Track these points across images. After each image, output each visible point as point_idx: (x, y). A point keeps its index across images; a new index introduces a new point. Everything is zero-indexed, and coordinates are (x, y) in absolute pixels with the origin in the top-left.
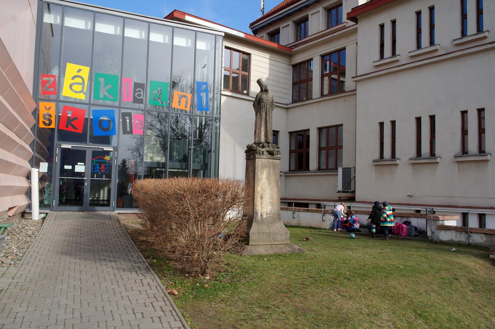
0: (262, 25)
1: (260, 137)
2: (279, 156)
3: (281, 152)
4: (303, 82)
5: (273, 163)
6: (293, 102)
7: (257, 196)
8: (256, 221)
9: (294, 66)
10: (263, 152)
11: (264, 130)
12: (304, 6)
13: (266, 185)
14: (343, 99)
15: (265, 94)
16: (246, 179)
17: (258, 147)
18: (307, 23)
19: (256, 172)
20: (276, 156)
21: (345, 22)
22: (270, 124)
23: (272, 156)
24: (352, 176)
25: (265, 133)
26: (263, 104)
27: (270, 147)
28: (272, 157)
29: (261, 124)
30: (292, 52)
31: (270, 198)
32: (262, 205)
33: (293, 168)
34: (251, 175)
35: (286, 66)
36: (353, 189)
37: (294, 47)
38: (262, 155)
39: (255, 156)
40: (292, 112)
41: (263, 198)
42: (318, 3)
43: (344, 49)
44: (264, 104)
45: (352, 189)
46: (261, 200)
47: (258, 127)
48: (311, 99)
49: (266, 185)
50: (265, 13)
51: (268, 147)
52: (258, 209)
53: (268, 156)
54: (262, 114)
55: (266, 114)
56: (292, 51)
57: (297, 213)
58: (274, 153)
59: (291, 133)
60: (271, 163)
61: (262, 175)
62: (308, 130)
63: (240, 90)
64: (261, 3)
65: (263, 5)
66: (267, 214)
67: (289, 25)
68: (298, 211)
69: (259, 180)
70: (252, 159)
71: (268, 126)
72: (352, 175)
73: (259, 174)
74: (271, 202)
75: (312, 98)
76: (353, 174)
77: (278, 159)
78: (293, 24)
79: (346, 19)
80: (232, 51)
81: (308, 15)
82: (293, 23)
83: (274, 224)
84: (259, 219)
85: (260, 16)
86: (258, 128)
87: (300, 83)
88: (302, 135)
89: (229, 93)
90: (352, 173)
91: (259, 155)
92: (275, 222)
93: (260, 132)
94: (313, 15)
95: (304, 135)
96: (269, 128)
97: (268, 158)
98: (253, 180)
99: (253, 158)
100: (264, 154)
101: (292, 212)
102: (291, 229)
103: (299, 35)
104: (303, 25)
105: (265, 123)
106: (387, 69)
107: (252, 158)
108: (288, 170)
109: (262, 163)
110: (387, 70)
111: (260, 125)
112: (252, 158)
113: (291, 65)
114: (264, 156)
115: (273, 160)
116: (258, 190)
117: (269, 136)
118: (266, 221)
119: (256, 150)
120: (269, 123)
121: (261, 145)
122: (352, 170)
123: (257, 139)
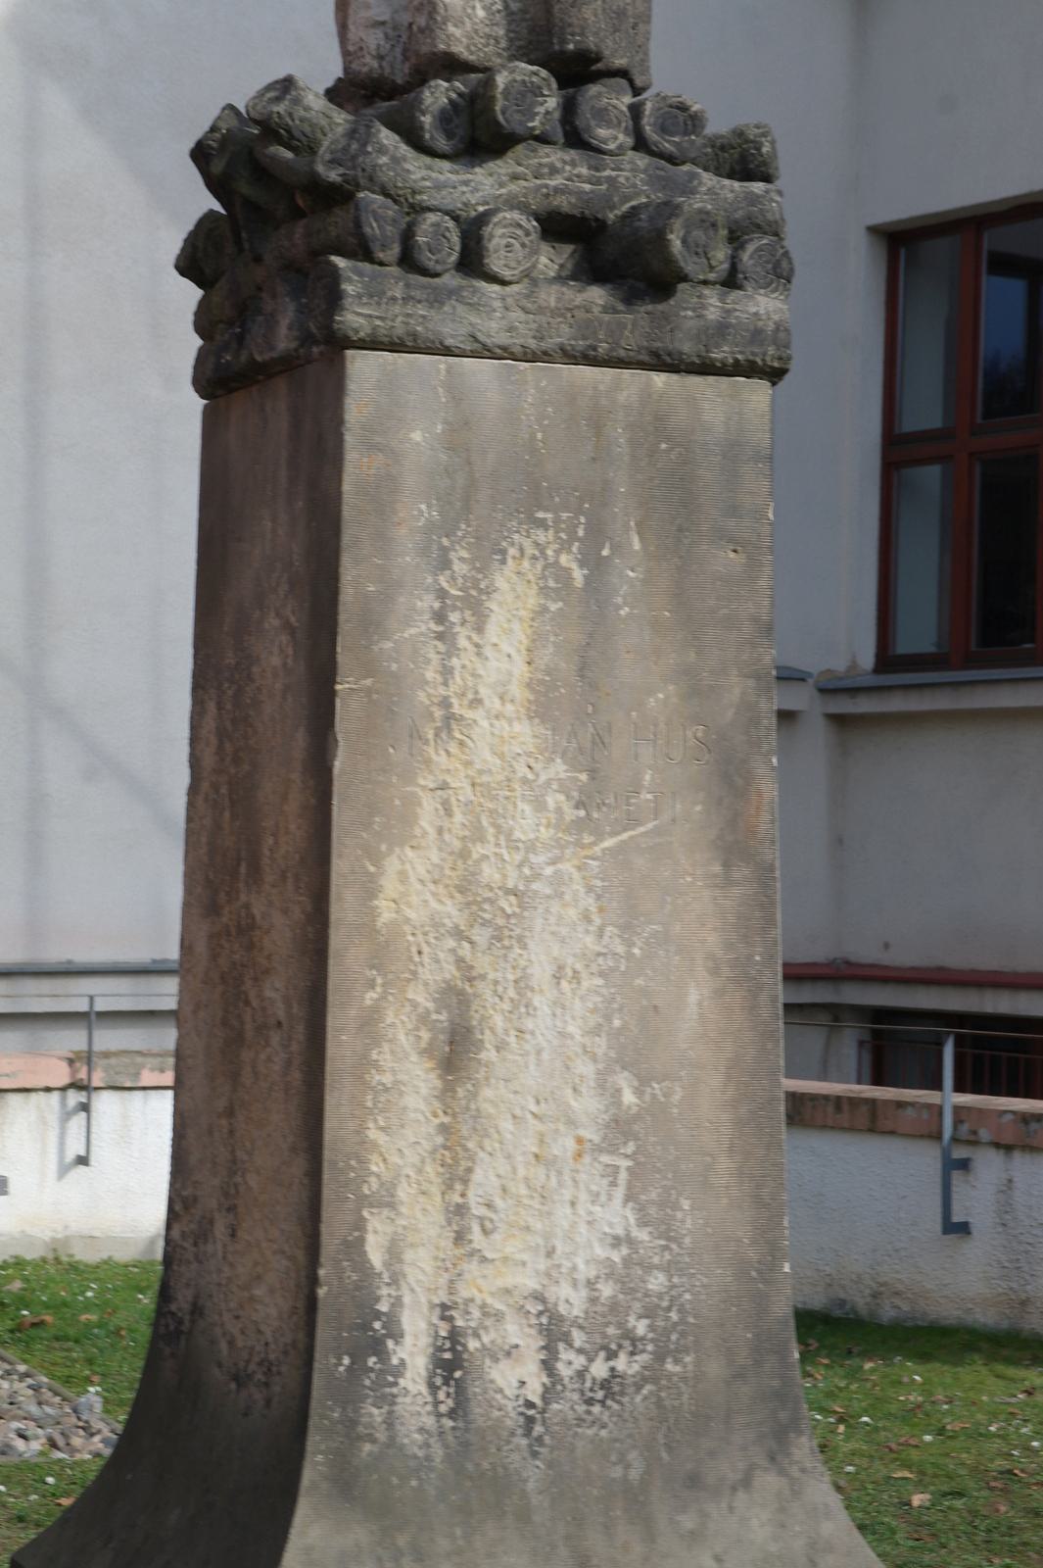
2: (763, 305)
3: (793, 241)
5: (654, 426)
7: (370, 1024)
8: (346, 1483)
10: (473, 233)
13: (526, 823)
16: (210, 723)
17: (386, 136)
19: (348, 594)
20: (714, 305)
23: (631, 299)
27: (612, 136)
28: (635, 326)
31: (601, 1045)
32: (456, 1174)
33: (919, 633)
38: (451, 280)
39: (334, 298)
41: (489, 1054)
46: (447, 1092)
49: (526, 823)
51: (576, 139)
52: (394, 1253)
53: (564, 311)
57: (989, 1167)
60: (619, 435)
61: (453, 650)
66: (553, 1332)
68: (1008, 1149)
69: (416, 735)
70: (287, 365)
74: (620, 1127)
77: (748, 369)
83: (688, 1522)
84: (411, 1437)
91: (395, 281)
92: (694, 1481)
97: (563, 334)
98: (301, 740)
99: (307, 339)
100: (496, 263)
102: (926, 1389)
107: (284, 340)
108: (867, 659)
109: (459, 436)
112: (284, 340)
115: (659, 379)
116: (386, 913)
118: (534, 1474)
119: (338, 196)
121: (438, 95)
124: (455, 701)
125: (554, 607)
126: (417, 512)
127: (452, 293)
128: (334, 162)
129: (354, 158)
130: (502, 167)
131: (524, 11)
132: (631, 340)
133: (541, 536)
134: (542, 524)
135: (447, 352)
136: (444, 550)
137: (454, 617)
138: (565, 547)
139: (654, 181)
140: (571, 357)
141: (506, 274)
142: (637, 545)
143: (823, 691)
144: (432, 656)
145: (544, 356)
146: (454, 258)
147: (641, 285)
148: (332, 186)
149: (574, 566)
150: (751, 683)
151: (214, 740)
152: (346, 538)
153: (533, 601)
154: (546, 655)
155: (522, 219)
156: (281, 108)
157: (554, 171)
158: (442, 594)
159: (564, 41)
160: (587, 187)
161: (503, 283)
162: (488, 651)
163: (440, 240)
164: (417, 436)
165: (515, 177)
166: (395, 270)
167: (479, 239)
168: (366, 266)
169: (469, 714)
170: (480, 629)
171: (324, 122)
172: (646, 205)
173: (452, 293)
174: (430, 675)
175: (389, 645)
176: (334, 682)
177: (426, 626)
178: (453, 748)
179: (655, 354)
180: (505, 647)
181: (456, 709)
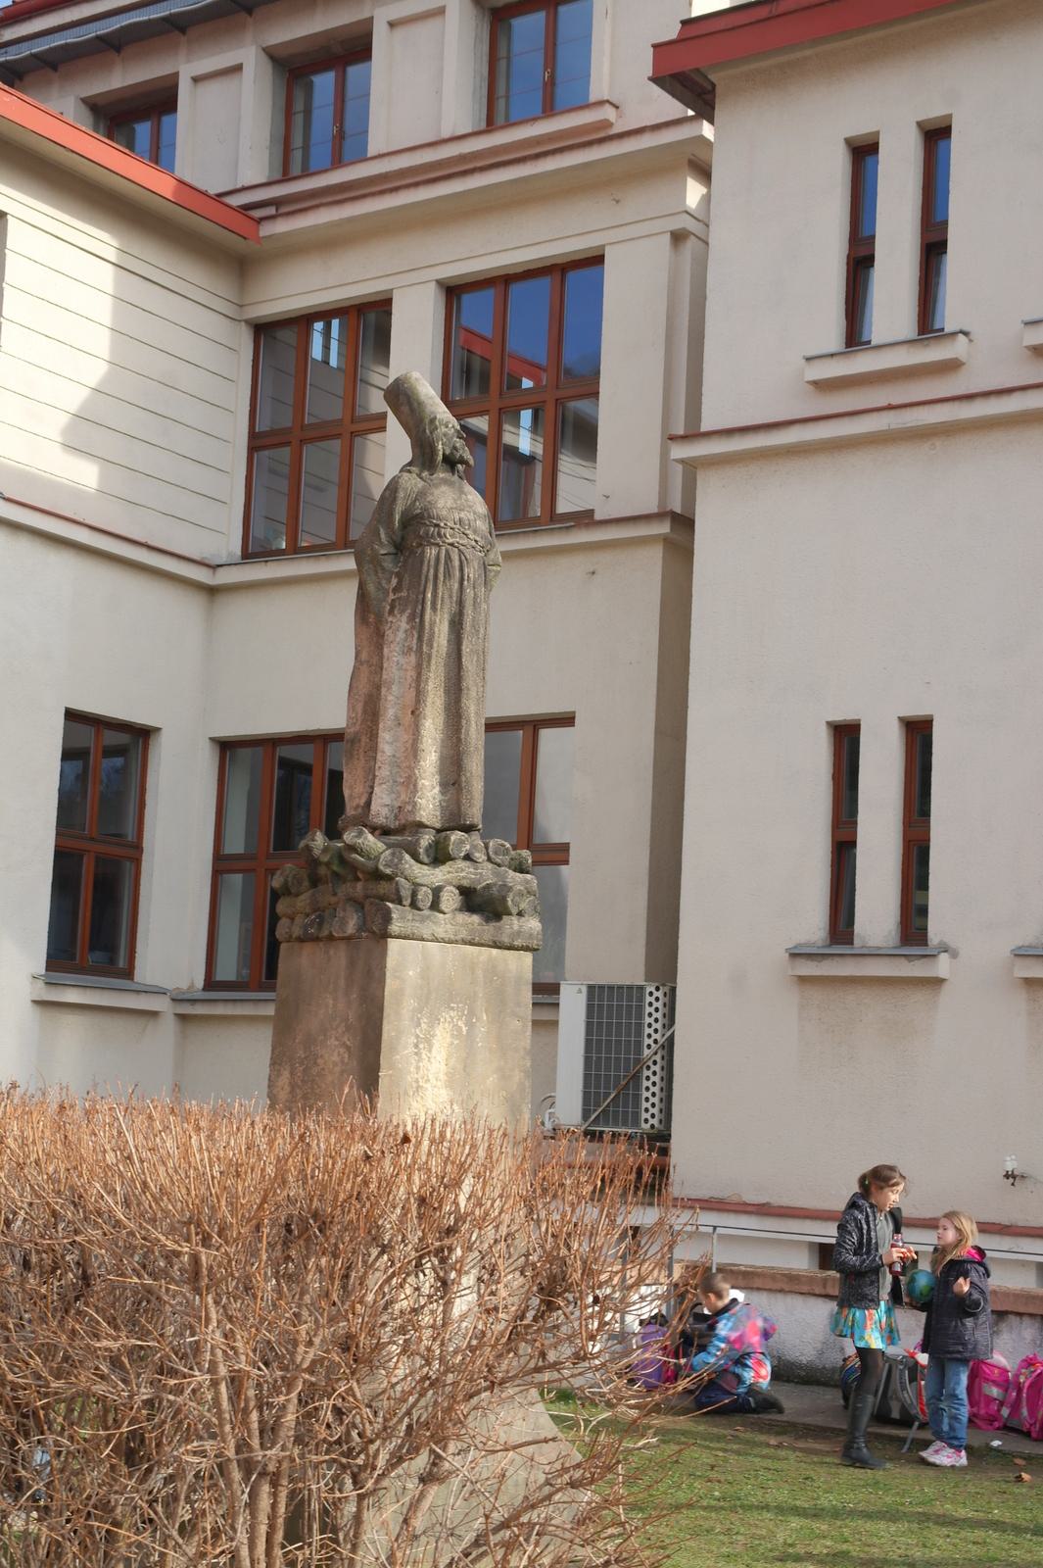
0: (58, 41)
4: (324, 432)
6: (252, 552)
9: (264, 331)
10: (437, 892)
11: (439, 736)
14: (581, 563)
15: (445, 481)
17: (407, 857)
21: (608, 101)
23: (488, 920)
24: (647, 1041)
25: (442, 759)
26: (434, 551)
28: (489, 930)
30: (259, 240)
33: (227, 971)
35: (214, 325)
36: (655, 1122)
37: (271, 211)
38: (427, 912)
40: (238, 612)
43: (596, 260)
45: (649, 1120)
54: (432, 624)
56: (262, 233)
58: (510, 903)
59: (227, 748)
60: (479, 973)
67: (237, 69)
69: (406, 1093)
70: (349, 938)
72: (647, 1031)
76: (658, 1026)
78: (267, 67)
79: (650, 79)
81: (369, 22)
82: (264, 59)
87: (303, 442)
90: (648, 1020)
93: (414, 751)
97: (464, 934)
99: (360, 929)
100: (443, 906)
103: (297, 140)
105: (447, 692)
106: (890, 408)
107: (351, 927)
108: (200, 983)
109: (425, 974)
110: (892, 413)
113: (247, 322)
115: (495, 951)
119: (390, 878)
120: (473, 693)
122: (648, 999)
124: (420, 1080)
125: (456, 1042)
126: (410, 1003)
127: (428, 917)
128: (387, 866)
129: (396, 865)
130: (445, 868)
131: (447, 807)
132: (487, 937)
133: (452, 1013)
134: (452, 1009)
135: (423, 940)
136: (419, 1019)
137: (421, 1046)
138: (460, 1018)
139: (494, 873)
140: (465, 942)
141: (446, 910)
142: (485, 1018)
143: (173, 1000)
144: (413, 1062)
145: (456, 942)
146: (429, 904)
147: (490, 915)
148: (387, 875)
149: (463, 1026)
150: (522, 1074)
151: (287, 1089)
152: (385, 1014)
153: (449, 1040)
154: (452, 1062)
155: (454, 889)
156: (360, 841)
157: (462, 870)
158: (417, 1036)
159: (465, 820)
160: (473, 876)
161: (444, 913)
162: (432, 1060)
163: (425, 896)
164: (411, 973)
165: (449, 872)
166: (408, 908)
167: (439, 897)
168: (399, 907)
169: (425, 1085)
170: (430, 1051)
171: (374, 846)
172: (495, 884)
173: (428, 917)
174: (412, 1069)
175: (398, 1057)
176: (378, 1072)
177: (411, 1049)
178: (419, 1099)
179: (495, 942)
180: (438, 1058)
181: (421, 1084)
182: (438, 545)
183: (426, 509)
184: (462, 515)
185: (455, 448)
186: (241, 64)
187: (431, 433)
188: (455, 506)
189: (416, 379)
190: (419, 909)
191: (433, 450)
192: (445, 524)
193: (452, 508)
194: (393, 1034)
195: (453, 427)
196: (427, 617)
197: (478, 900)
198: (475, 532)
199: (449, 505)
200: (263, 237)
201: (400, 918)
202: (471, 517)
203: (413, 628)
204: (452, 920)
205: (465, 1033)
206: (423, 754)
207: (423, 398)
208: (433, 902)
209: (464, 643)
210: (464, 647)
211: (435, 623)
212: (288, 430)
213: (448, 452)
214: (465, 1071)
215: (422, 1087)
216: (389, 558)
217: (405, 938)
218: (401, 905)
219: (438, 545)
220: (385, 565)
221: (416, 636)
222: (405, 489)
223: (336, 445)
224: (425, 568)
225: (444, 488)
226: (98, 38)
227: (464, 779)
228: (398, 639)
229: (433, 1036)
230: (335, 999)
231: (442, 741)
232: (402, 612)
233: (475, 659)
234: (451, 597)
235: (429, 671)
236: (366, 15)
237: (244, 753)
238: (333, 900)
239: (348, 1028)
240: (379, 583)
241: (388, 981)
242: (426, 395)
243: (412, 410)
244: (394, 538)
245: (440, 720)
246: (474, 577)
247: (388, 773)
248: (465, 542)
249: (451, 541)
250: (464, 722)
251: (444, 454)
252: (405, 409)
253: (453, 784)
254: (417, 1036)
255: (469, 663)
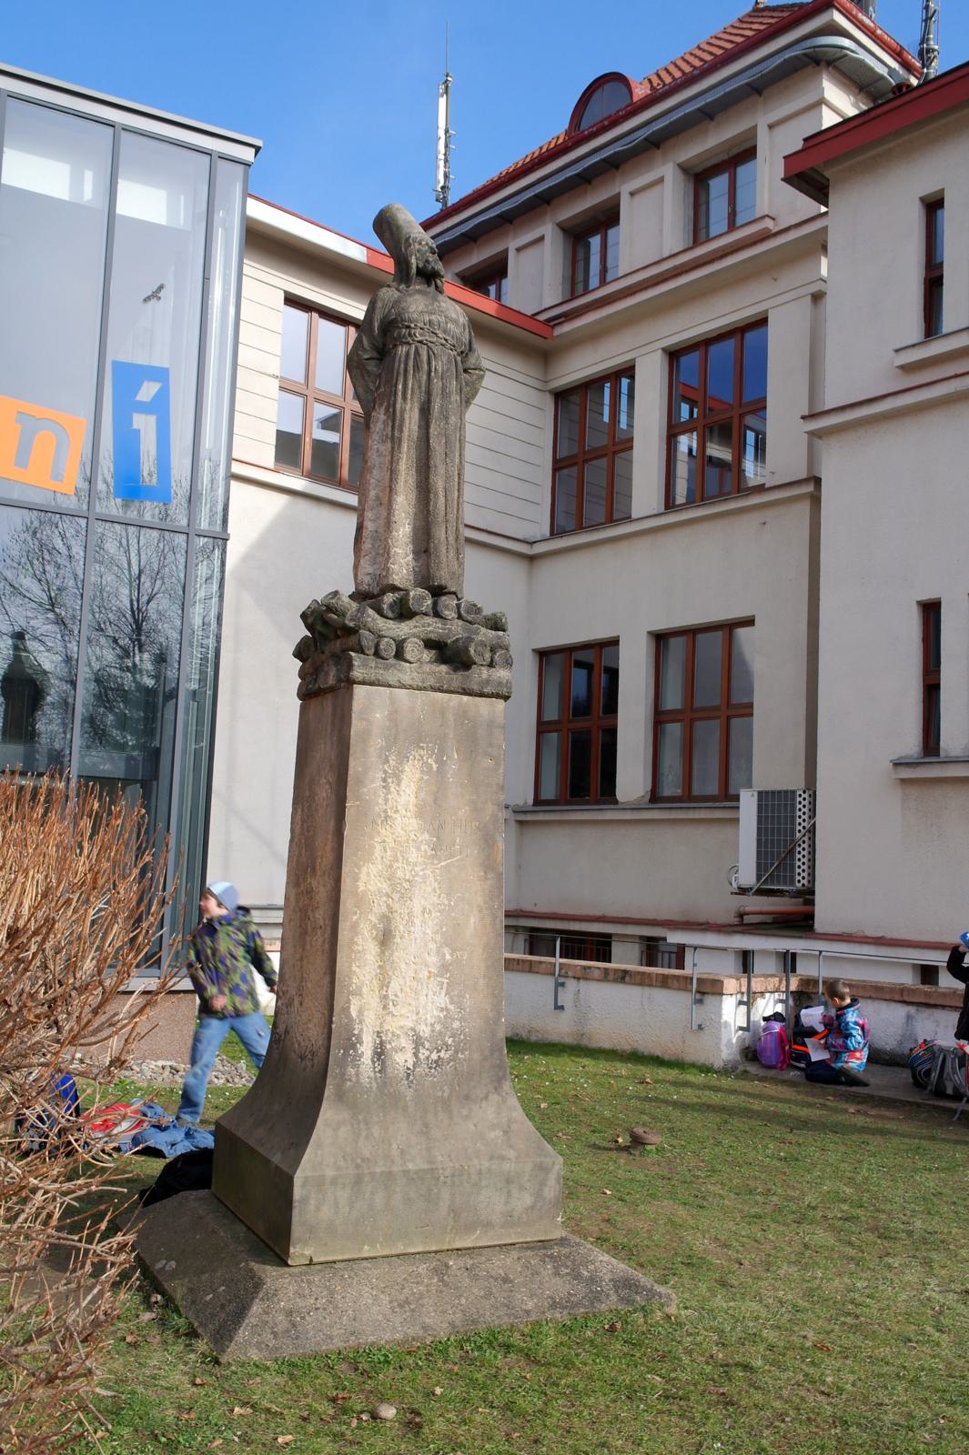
1: (384, 553)
2: (502, 674)
4: (597, 454)
5: (463, 714)
6: (556, 532)
7: (354, 928)
8: (340, 1096)
9: (561, 396)
11: (412, 510)
12: (604, 160)
13: (414, 856)
14: (757, 517)
15: (419, 292)
16: (298, 817)
17: (371, 612)
18: (611, 232)
19: (351, 771)
20: (485, 672)
21: (767, 216)
22: (448, 478)
23: (456, 670)
24: (798, 828)
25: (415, 530)
28: (457, 679)
29: (393, 473)
31: (438, 937)
32: (384, 983)
33: (549, 792)
34: (324, 793)
36: (805, 882)
37: (563, 319)
38: (392, 661)
39: (350, 667)
40: (547, 570)
41: (397, 940)
42: (658, 148)
43: (761, 322)
44: (417, 353)
45: (801, 881)
46: (382, 952)
47: (372, 494)
48: (628, 518)
49: (414, 856)
50: (453, 199)
51: (437, 614)
52: (360, 1012)
54: (403, 411)
55: (425, 411)
57: (571, 985)
58: (472, 652)
59: (543, 655)
60: (450, 717)
61: (389, 792)
62: (614, 643)
63: (345, 473)
64: (437, 167)
65: (446, 176)
66: (418, 1042)
67: (542, 238)
68: (579, 979)
69: (374, 822)
70: (332, 689)
71: (438, 483)
72: (798, 820)
73: (373, 784)
74: (444, 968)
75: (630, 517)
76: (806, 817)
77: (497, 696)
78: (560, 235)
79: (782, 180)
80: (315, 315)
82: (557, 230)
83: (465, 1112)
84: (365, 1080)
85: (436, 208)
86: (378, 498)
87: (585, 461)
88: (588, 667)
89: (299, 484)
90: (798, 813)
91: (372, 661)
92: (467, 1097)
93: (388, 524)
94: (638, 198)
95: (596, 668)
96: (442, 500)
97: (431, 681)
98: (332, 823)
99: (340, 680)
100: (408, 656)
101: (549, 983)
102: (547, 1066)
103: (580, 277)
104: (595, 241)
105: (418, 471)
106: (957, 376)
107: (331, 681)
108: (531, 801)
109: (393, 716)
110: (958, 380)
111: (388, 477)
112: (331, 681)
113: (550, 391)
114: (407, 673)
115: (465, 698)
116: (361, 888)
117: (443, 550)
118: (409, 1094)
119: (353, 631)
120: (441, 470)
121: (389, 598)
122: (798, 799)
123: (366, 567)
124: (389, 811)
126: (377, 742)
127: (392, 666)
130: (411, 623)
131: (420, 572)
132: (455, 685)
133: (422, 752)
134: (422, 748)
135: (390, 686)
137: (390, 780)
138: (430, 756)
139: (465, 630)
140: (434, 689)
141: (412, 660)
142: (456, 757)
143: (514, 812)
144: (381, 793)
145: (425, 689)
148: (351, 627)
151: (300, 823)
152: (351, 751)
153: (418, 775)
154: (423, 795)
156: (334, 601)
157: (429, 625)
158: (385, 772)
159: (433, 582)
161: (410, 663)
162: (401, 793)
163: (388, 647)
164: (378, 715)
165: (416, 627)
166: (372, 657)
168: (362, 656)
169: (394, 816)
170: (399, 785)
173: (392, 666)
174: (380, 801)
175: (365, 790)
177: (379, 783)
178: (388, 827)
179: (464, 689)
180: (408, 791)
181: (389, 814)
182: (408, 343)
183: (399, 314)
184: (433, 317)
185: (427, 261)
186: (543, 236)
187: (406, 250)
188: (425, 310)
189: (397, 209)
190: (383, 658)
191: (408, 264)
192: (415, 325)
193: (422, 312)
194: (360, 769)
195: (427, 244)
196: (398, 406)
197: (448, 653)
198: (445, 332)
199: (420, 308)
200: (557, 336)
201: (361, 667)
202: (442, 319)
203: (388, 417)
204: (421, 664)
205: (435, 769)
206: (394, 525)
207: (401, 222)
208: (396, 652)
209: (432, 426)
210: (431, 430)
211: (405, 410)
212: (575, 456)
213: (421, 265)
214: (435, 803)
215: (390, 817)
216: (372, 363)
217: (371, 684)
218: (364, 654)
219: (408, 343)
220: (369, 368)
221: (390, 424)
222: (383, 300)
223: (603, 462)
224: (397, 364)
225: (417, 297)
226: (462, 234)
227: (432, 545)
228: (377, 430)
229: (402, 772)
230: (325, 744)
231: (415, 514)
232: (381, 405)
233: (444, 441)
234: (420, 387)
235: (400, 453)
236: (617, 191)
237: (558, 658)
238: (323, 657)
239: (331, 766)
240: (367, 386)
241: (355, 722)
242: (405, 219)
243: (392, 234)
244: (376, 344)
245: (413, 496)
246: (443, 370)
247: (370, 546)
248: (435, 339)
249: (420, 339)
250: (432, 496)
251: (417, 267)
252: (387, 234)
253: (425, 552)
254: (385, 772)
255: (437, 445)
